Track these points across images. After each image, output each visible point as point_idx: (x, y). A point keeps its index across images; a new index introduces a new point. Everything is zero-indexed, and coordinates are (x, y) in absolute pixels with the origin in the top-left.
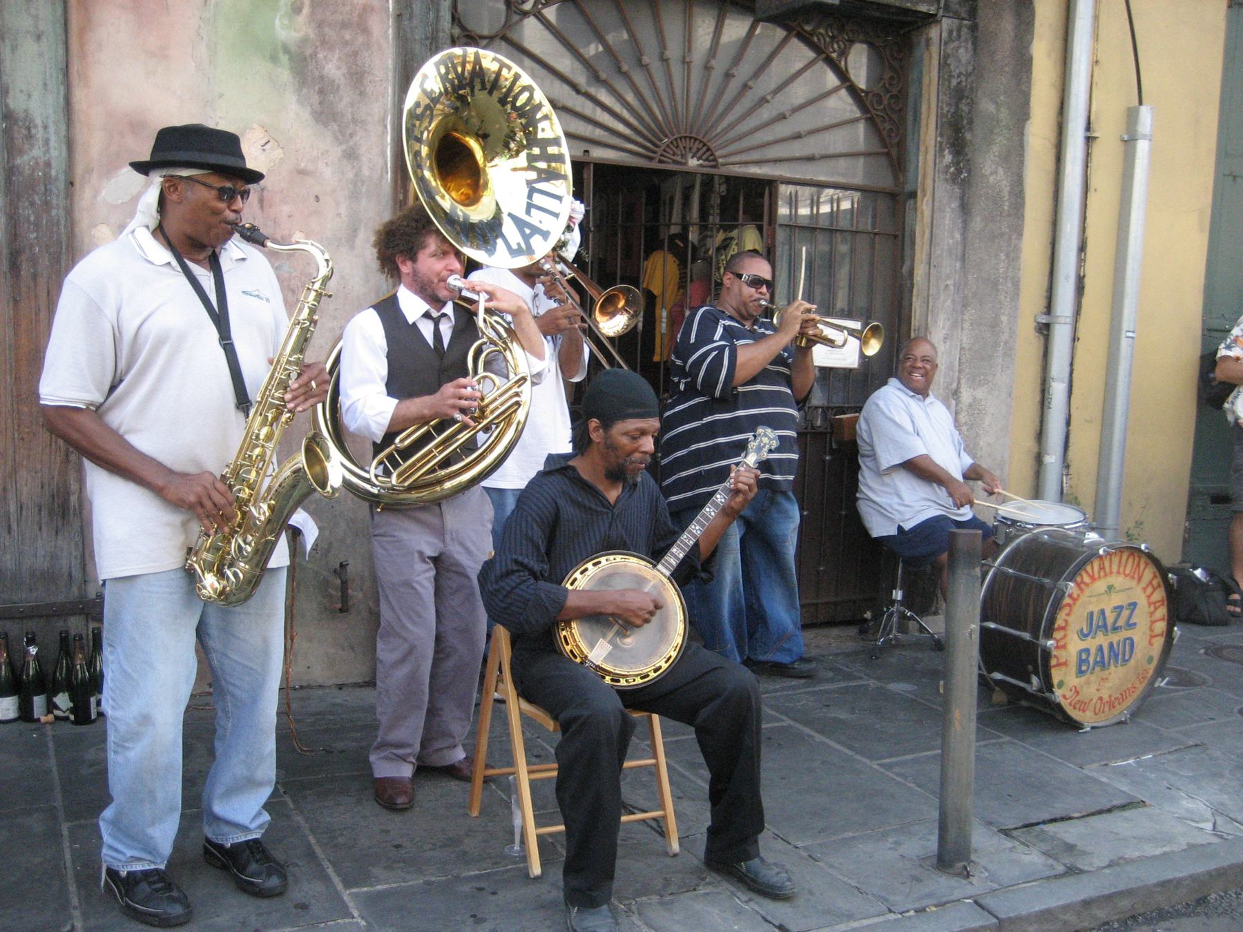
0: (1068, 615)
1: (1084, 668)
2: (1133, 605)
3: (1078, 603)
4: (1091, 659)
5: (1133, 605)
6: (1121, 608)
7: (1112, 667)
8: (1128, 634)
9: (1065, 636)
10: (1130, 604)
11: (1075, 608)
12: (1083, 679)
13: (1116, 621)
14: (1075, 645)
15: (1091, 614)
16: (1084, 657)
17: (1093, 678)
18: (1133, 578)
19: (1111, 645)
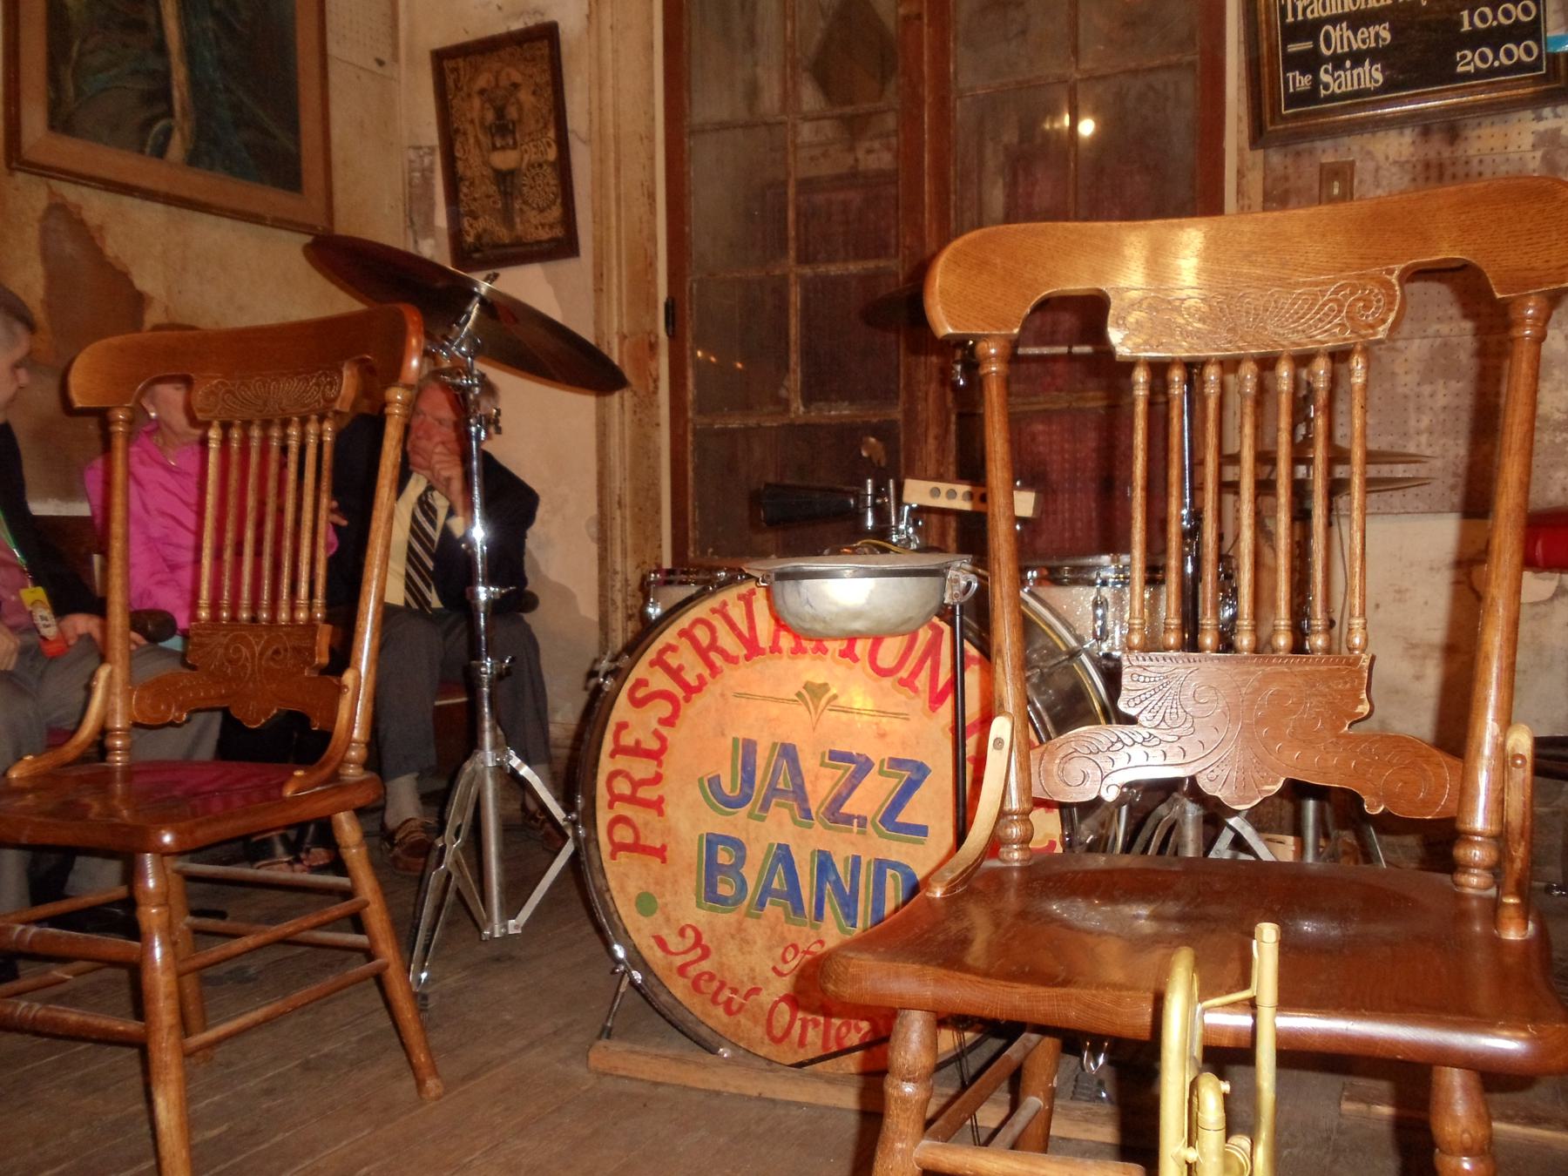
0: (669, 722)
1: (725, 890)
2: (914, 776)
3: (699, 701)
6: (862, 766)
8: (897, 850)
9: (657, 779)
10: (897, 763)
11: (689, 711)
12: (725, 919)
13: (839, 800)
14: (688, 820)
15: (749, 747)
16: (724, 857)
19: (824, 863)
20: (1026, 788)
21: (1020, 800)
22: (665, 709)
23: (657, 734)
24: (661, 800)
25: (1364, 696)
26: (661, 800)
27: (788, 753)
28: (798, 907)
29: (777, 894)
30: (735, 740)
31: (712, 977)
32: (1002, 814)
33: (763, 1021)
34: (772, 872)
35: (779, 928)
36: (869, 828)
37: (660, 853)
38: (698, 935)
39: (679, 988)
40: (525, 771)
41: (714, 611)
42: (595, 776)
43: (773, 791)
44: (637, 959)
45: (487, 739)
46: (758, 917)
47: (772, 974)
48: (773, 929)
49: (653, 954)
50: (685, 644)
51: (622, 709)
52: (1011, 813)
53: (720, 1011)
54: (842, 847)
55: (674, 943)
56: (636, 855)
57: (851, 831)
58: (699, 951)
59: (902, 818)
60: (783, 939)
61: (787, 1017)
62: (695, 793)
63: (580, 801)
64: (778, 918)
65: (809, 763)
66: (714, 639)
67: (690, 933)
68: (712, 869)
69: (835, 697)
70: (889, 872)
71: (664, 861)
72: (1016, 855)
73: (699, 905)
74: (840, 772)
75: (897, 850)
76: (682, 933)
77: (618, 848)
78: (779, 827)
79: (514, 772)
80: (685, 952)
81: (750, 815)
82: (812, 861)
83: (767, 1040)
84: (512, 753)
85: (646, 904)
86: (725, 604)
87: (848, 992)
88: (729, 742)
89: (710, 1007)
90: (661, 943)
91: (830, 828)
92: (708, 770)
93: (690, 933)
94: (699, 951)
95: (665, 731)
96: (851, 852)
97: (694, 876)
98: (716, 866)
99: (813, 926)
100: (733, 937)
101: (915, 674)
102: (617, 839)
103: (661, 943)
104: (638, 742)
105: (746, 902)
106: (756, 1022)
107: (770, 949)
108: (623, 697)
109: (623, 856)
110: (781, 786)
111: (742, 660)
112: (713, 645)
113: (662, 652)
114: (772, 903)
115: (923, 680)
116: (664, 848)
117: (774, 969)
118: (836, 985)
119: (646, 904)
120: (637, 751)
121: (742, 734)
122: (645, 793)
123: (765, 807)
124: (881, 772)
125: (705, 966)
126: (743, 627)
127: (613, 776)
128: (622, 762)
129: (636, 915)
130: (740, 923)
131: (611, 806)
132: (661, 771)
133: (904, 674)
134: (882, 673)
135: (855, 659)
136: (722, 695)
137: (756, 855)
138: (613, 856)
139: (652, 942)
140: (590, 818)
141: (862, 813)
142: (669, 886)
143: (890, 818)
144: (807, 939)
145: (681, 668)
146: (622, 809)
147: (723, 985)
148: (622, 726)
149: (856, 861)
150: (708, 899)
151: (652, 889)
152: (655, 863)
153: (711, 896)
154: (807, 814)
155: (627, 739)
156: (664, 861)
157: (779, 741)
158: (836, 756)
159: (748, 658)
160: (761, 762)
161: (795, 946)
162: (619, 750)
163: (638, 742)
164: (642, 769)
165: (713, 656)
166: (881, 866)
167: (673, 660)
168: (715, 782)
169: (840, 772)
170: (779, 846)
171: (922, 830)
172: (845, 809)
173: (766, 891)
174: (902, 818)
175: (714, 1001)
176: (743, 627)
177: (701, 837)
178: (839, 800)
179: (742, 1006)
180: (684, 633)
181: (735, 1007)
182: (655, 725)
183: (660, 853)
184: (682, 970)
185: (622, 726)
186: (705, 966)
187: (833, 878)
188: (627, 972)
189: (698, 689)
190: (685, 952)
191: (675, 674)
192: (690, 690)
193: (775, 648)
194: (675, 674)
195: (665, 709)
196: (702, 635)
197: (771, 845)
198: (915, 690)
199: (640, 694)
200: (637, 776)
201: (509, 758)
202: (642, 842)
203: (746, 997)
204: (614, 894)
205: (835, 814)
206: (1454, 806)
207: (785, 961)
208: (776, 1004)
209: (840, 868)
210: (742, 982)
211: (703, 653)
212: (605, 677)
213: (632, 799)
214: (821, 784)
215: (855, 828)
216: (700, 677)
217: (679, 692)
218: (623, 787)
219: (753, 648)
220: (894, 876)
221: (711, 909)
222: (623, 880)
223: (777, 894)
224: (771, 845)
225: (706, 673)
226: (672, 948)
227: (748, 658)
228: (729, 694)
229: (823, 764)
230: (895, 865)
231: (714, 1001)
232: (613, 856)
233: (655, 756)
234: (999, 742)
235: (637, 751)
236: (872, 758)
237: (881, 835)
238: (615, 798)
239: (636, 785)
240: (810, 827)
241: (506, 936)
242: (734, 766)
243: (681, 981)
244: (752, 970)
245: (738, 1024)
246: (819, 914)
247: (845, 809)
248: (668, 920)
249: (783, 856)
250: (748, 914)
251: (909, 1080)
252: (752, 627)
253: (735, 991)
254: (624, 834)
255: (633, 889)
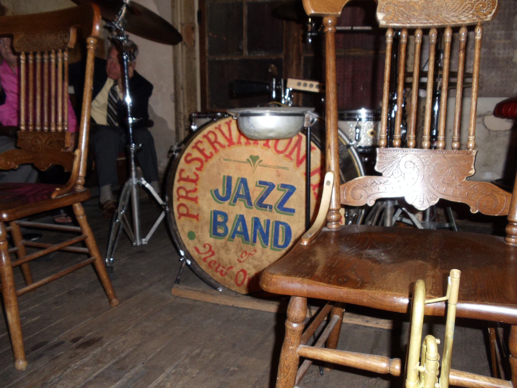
0: (199, 169)
1: (220, 231)
2: (290, 190)
3: (211, 161)
4: (230, 225)
5: (290, 190)
6: (271, 186)
7: (259, 245)
8: (283, 218)
9: (195, 190)
10: (284, 186)
12: (220, 242)
14: (207, 205)
15: (229, 179)
16: (220, 219)
17: (230, 245)
18: (289, 156)
19: (256, 222)
20: (338, 200)
21: (336, 205)
22: (198, 164)
23: (195, 173)
24: (197, 198)
25: (473, 167)
26: (197, 198)
27: (244, 181)
28: (247, 238)
29: (239, 233)
30: (224, 176)
31: (215, 262)
32: (329, 210)
33: (234, 278)
34: (237, 225)
35: (240, 245)
36: (273, 210)
37: (196, 217)
38: (211, 247)
39: (203, 266)
40: (148, 186)
41: (216, 128)
42: (172, 189)
43: (238, 195)
44: (188, 255)
45: (134, 174)
46: (232, 241)
47: (237, 262)
48: (238, 245)
49: (194, 254)
50: (205, 140)
51: (182, 164)
52: (333, 210)
53: (218, 274)
54: (263, 216)
55: (202, 250)
56: (187, 218)
57: (267, 210)
58: (211, 253)
59: (286, 206)
60: (241, 249)
61: (243, 277)
62: (209, 195)
63: (167, 198)
64: (239, 242)
65: (251, 185)
66: (216, 138)
67: (207, 246)
68: (215, 224)
69: (261, 161)
70: (281, 226)
71: (198, 220)
72: (334, 226)
73: (211, 236)
74: (263, 189)
75: (283, 218)
76: (204, 246)
77: (181, 215)
78: (239, 209)
79: (143, 187)
80: (206, 253)
81: (230, 204)
82: (252, 221)
83: (235, 285)
84: (143, 179)
85: (191, 235)
86: (220, 126)
87: (272, 289)
88: (222, 177)
89: (215, 273)
90: (197, 250)
91: (258, 209)
92: (213, 188)
93: (207, 246)
94: (211, 253)
95: (198, 172)
96: (266, 218)
97: (209, 226)
98: (217, 223)
99: (252, 245)
100: (223, 248)
101: (291, 153)
102: (180, 211)
103: (197, 250)
104: (188, 177)
105: (228, 236)
106: (231, 278)
107: (236, 253)
108: (182, 160)
109: (183, 218)
110: (241, 193)
111: (227, 147)
112: (216, 141)
113: (197, 143)
114: (237, 236)
115: (294, 155)
116: (198, 215)
117: (238, 260)
118: (267, 285)
119: (191, 235)
120: (187, 180)
121: (226, 174)
122: (190, 195)
123: (235, 201)
124: (278, 189)
125: (213, 258)
126: (227, 134)
127: (179, 188)
128: (182, 184)
129: (187, 239)
130: (226, 243)
131: (178, 200)
132: (197, 187)
133: (287, 153)
134: (279, 152)
135: (269, 147)
136: (219, 159)
137: (232, 219)
138: (179, 218)
139: (194, 249)
140: (170, 203)
141: (271, 204)
142: (199, 229)
143: (281, 206)
144: (250, 249)
145: (204, 149)
146: (182, 201)
147: (219, 265)
148: (182, 170)
149: (268, 222)
150: (214, 234)
151: (194, 230)
152: (195, 221)
153: (215, 233)
154: (250, 203)
155: (184, 175)
156: (198, 220)
157: (240, 177)
158: (262, 183)
159: (229, 146)
160: (234, 184)
161: (246, 252)
162: (181, 179)
163: (188, 177)
164: (190, 186)
165: (216, 145)
166: (277, 223)
167: (200, 146)
168: (216, 191)
169: (263, 189)
170: (240, 215)
171: (292, 211)
172: (265, 202)
173: (235, 232)
174: (286, 206)
175: (216, 270)
176: (227, 134)
177: (211, 211)
178: (262, 199)
179: (226, 273)
180: (205, 136)
181: (224, 273)
182: (194, 170)
183: (196, 217)
184: (205, 260)
185: (182, 170)
186: (213, 258)
187: (260, 227)
188: (185, 260)
189: (210, 157)
190: (206, 253)
191: (202, 151)
192: (207, 158)
193: (239, 143)
194: (202, 151)
195: (198, 164)
196: (212, 137)
197: (237, 215)
198: (291, 159)
199: (189, 158)
200: (188, 189)
201: (142, 181)
202: (190, 213)
203: (228, 269)
204: (180, 231)
205: (261, 204)
206: (507, 211)
207: (242, 257)
208: (238, 272)
209: (262, 224)
210: (226, 264)
211: (212, 144)
212: (176, 152)
213: (186, 198)
214: (256, 193)
215: (268, 209)
216: (211, 153)
217: (203, 158)
218: (183, 193)
219: (231, 142)
220: (282, 227)
221: (215, 238)
222: (183, 227)
223: (239, 233)
224: (237, 215)
225: (213, 151)
226: (201, 252)
227: (229, 146)
228: (222, 159)
229: (256, 186)
230: (283, 223)
231: (216, 270)
232: (179, 218)
233: (195, 181)
234: (328, 183)
235: (187, 180)
236: (275, 183)
237: (278, 212)
238: (180, 197)
239: (187, 192)
240: (252, 208)
241: (142, 245)
242: (224, 186)
243: (204, 263)
244: (230, 260)
245: (225, 279)
246: (255, 241)
247: (265, 202)
248: (199, 241)
249: (241, 219)
250: (228, 240)
251: (295, 323)
252: (230, 134)
253: (224, 267)
254: (183, 210)
255: (187, 229)
